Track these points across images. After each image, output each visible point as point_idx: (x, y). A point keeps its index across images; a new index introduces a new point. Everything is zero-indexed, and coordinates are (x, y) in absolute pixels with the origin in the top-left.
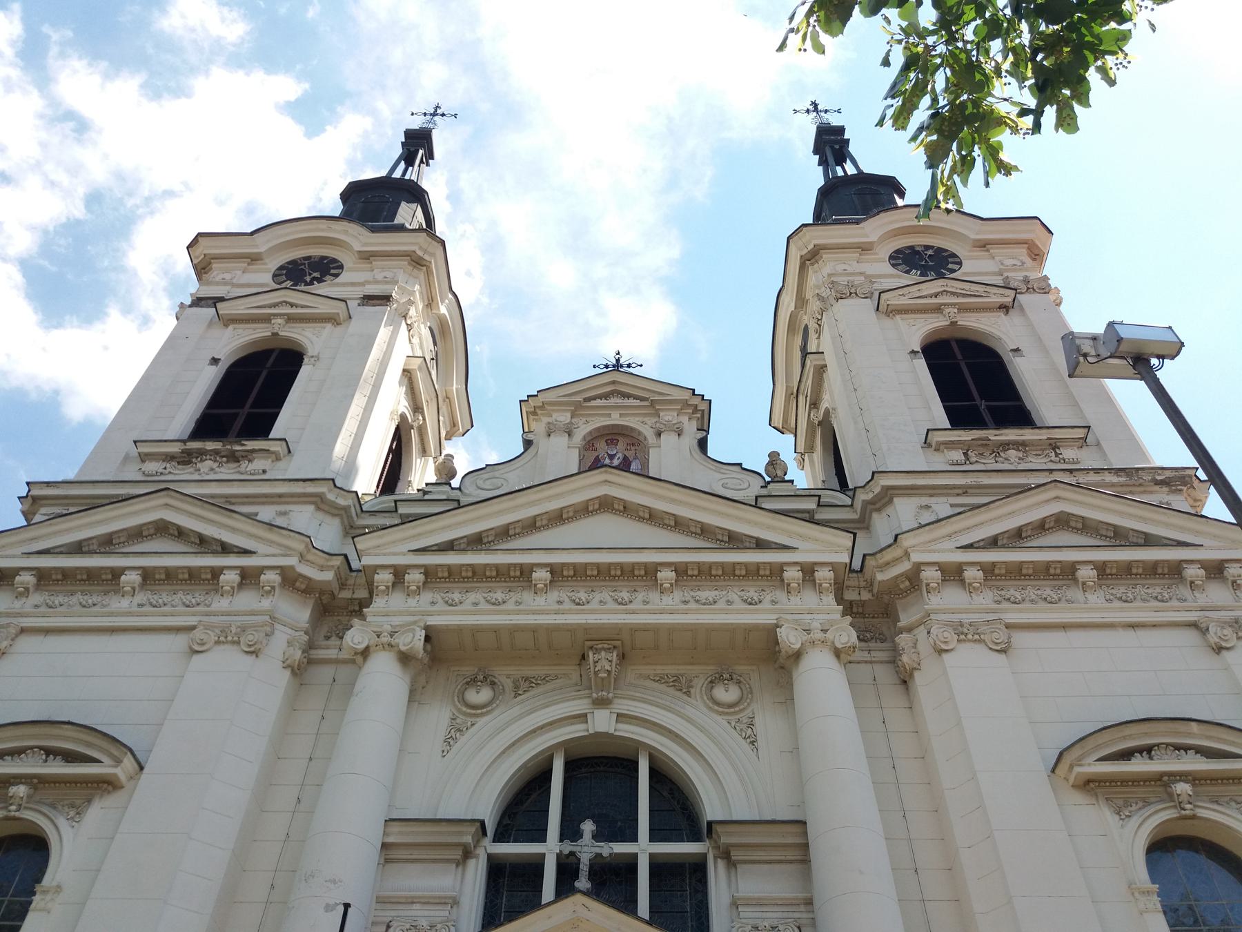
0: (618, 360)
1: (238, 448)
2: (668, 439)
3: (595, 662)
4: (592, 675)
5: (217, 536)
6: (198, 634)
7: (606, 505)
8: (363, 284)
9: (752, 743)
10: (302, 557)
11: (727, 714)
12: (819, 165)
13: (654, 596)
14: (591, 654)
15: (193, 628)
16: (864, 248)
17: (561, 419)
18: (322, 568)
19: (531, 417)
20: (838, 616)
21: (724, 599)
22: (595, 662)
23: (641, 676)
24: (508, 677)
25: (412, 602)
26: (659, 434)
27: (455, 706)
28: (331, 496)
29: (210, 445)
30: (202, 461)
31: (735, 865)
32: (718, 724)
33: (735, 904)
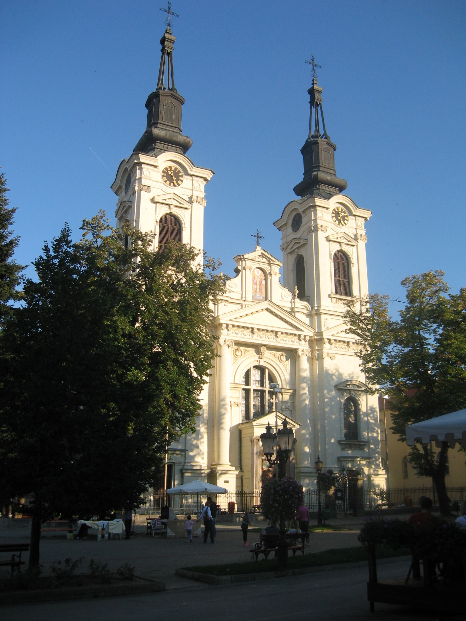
0: (258, 234)
7: (267, 309)
12: (309, 103)
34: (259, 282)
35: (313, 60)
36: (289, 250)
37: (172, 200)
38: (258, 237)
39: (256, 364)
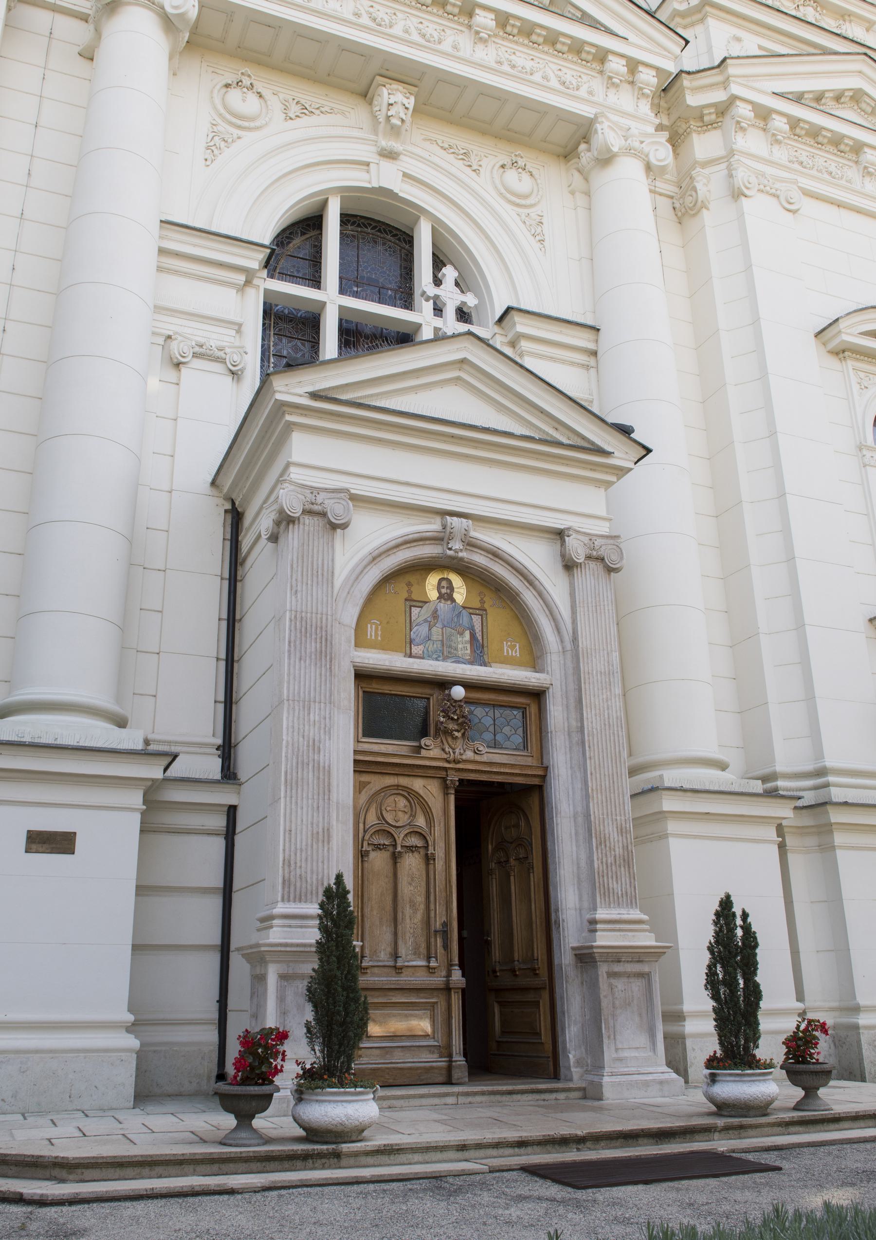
4: (382, 119)
9: (541, 241)
11: (518, 205)
14: (385, 91)
20: (651, 130)
21: (540, 73)
32: (508, 212)
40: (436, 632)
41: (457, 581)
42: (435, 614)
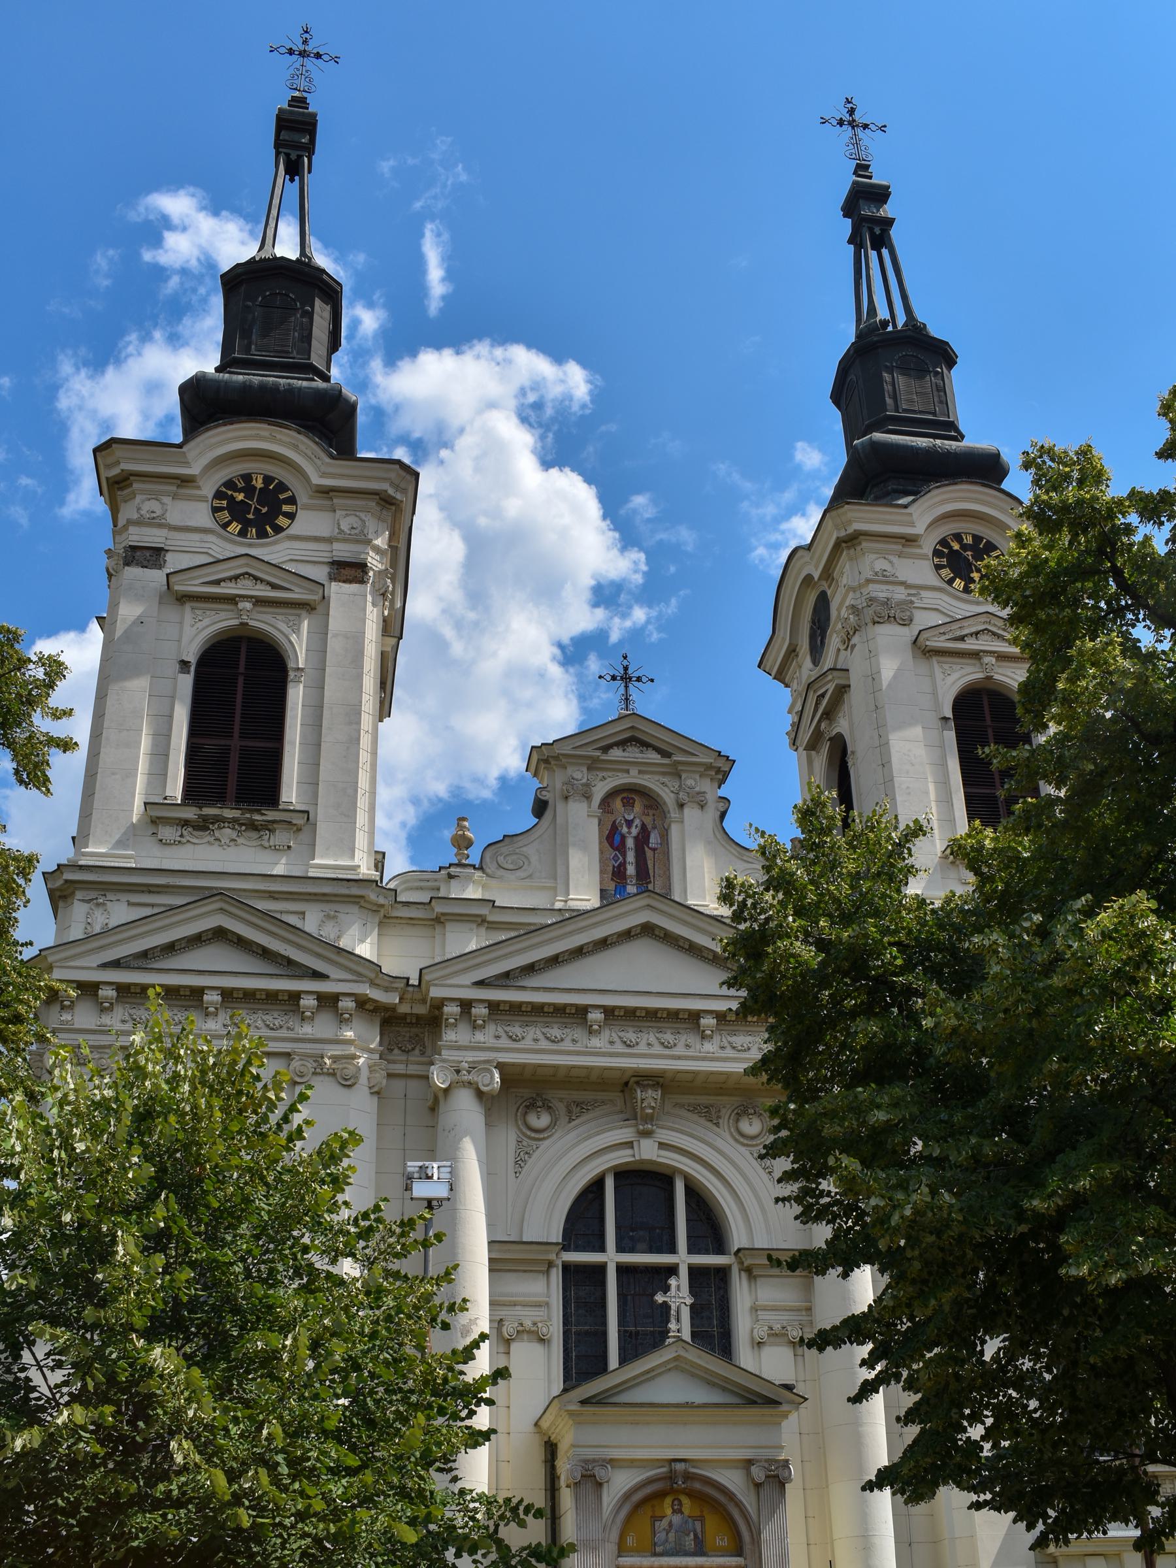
0: (626, 669)
1: (257, 817)
2: (690, 813)
3: (643, 1100)
5: (283, 952)
6: (296, 1064)
7: (648, 930)
8: (329, 540)
10: (373, 984)
13: (693, 1039)
15: (287, 1055)
16: (910, 540)
17: (578, 775)
18: (387, 990)
19: (543, 766)
22: (643, 1100)
23: (676, 1105)
24: (561, 1100)
25: (479, 1037)
26: (681, 806)
27: (518, 1126)
28: (373, 896)
29: (229, 813)
30: (220, 828)
31: (755, 1277)
33: (755, 1309)
34: (636, 838)
35: (852, 112)
36: (805, 737)
37: (248, 583)
38: (626, 679)
39: (622, 1157)
40: (672, 1535)
41: (686, 1501)
42: (670, 1524)
